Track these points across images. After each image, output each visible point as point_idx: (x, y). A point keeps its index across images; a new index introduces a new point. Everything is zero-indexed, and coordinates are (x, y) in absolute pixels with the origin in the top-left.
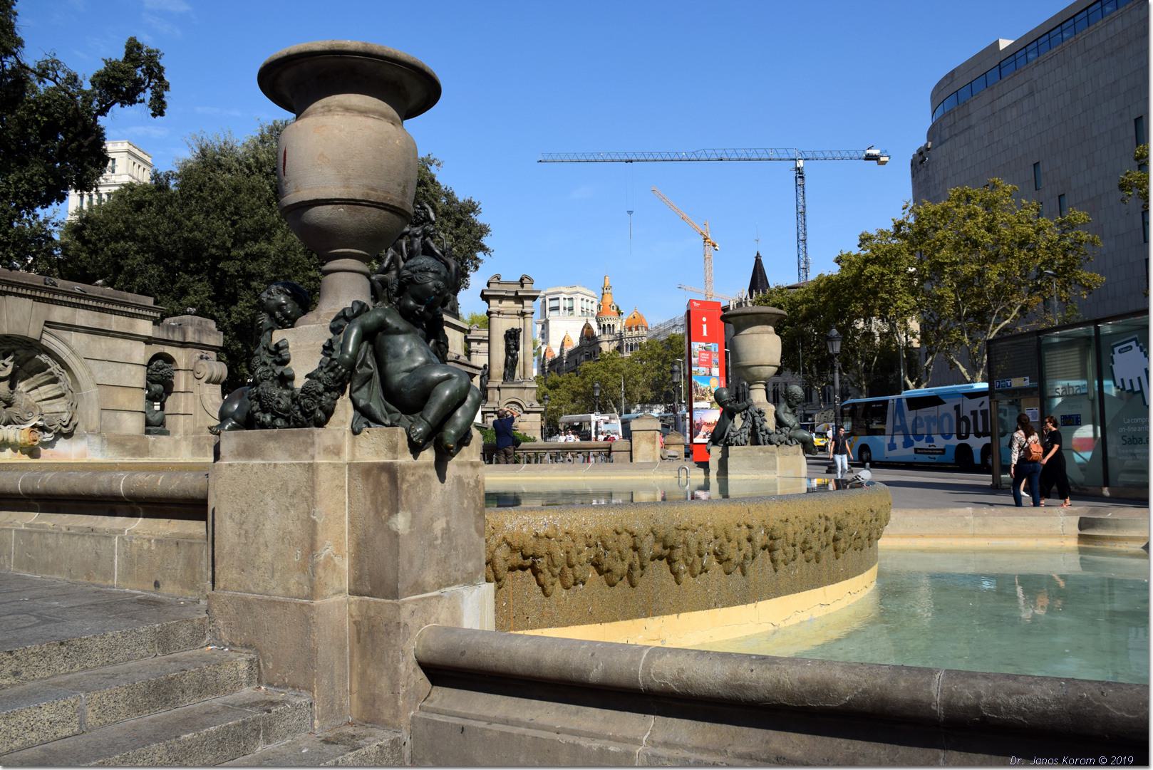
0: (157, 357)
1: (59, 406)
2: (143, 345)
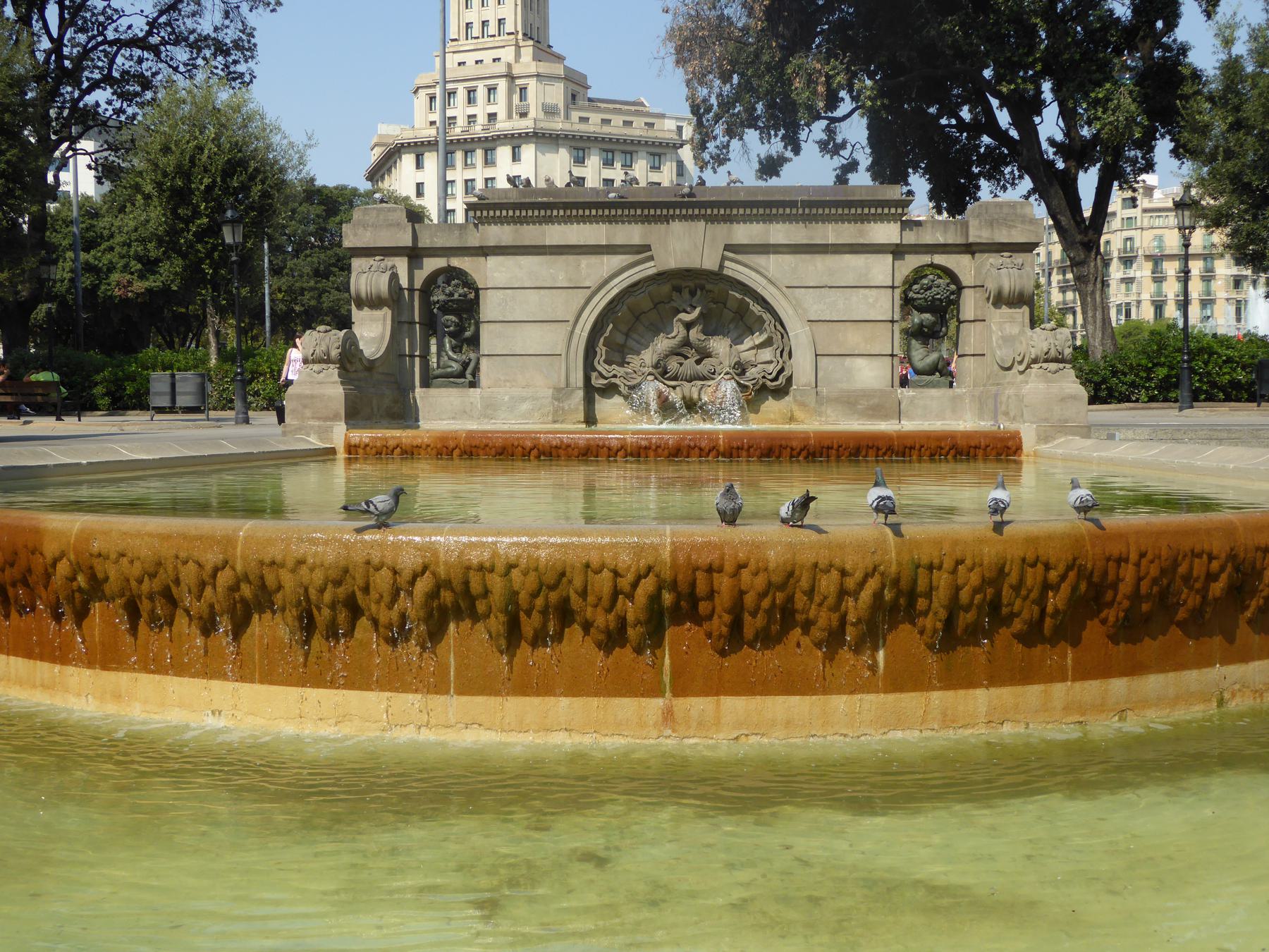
0: (918, 274)
1: (767, 354)
2: (890, 257)
